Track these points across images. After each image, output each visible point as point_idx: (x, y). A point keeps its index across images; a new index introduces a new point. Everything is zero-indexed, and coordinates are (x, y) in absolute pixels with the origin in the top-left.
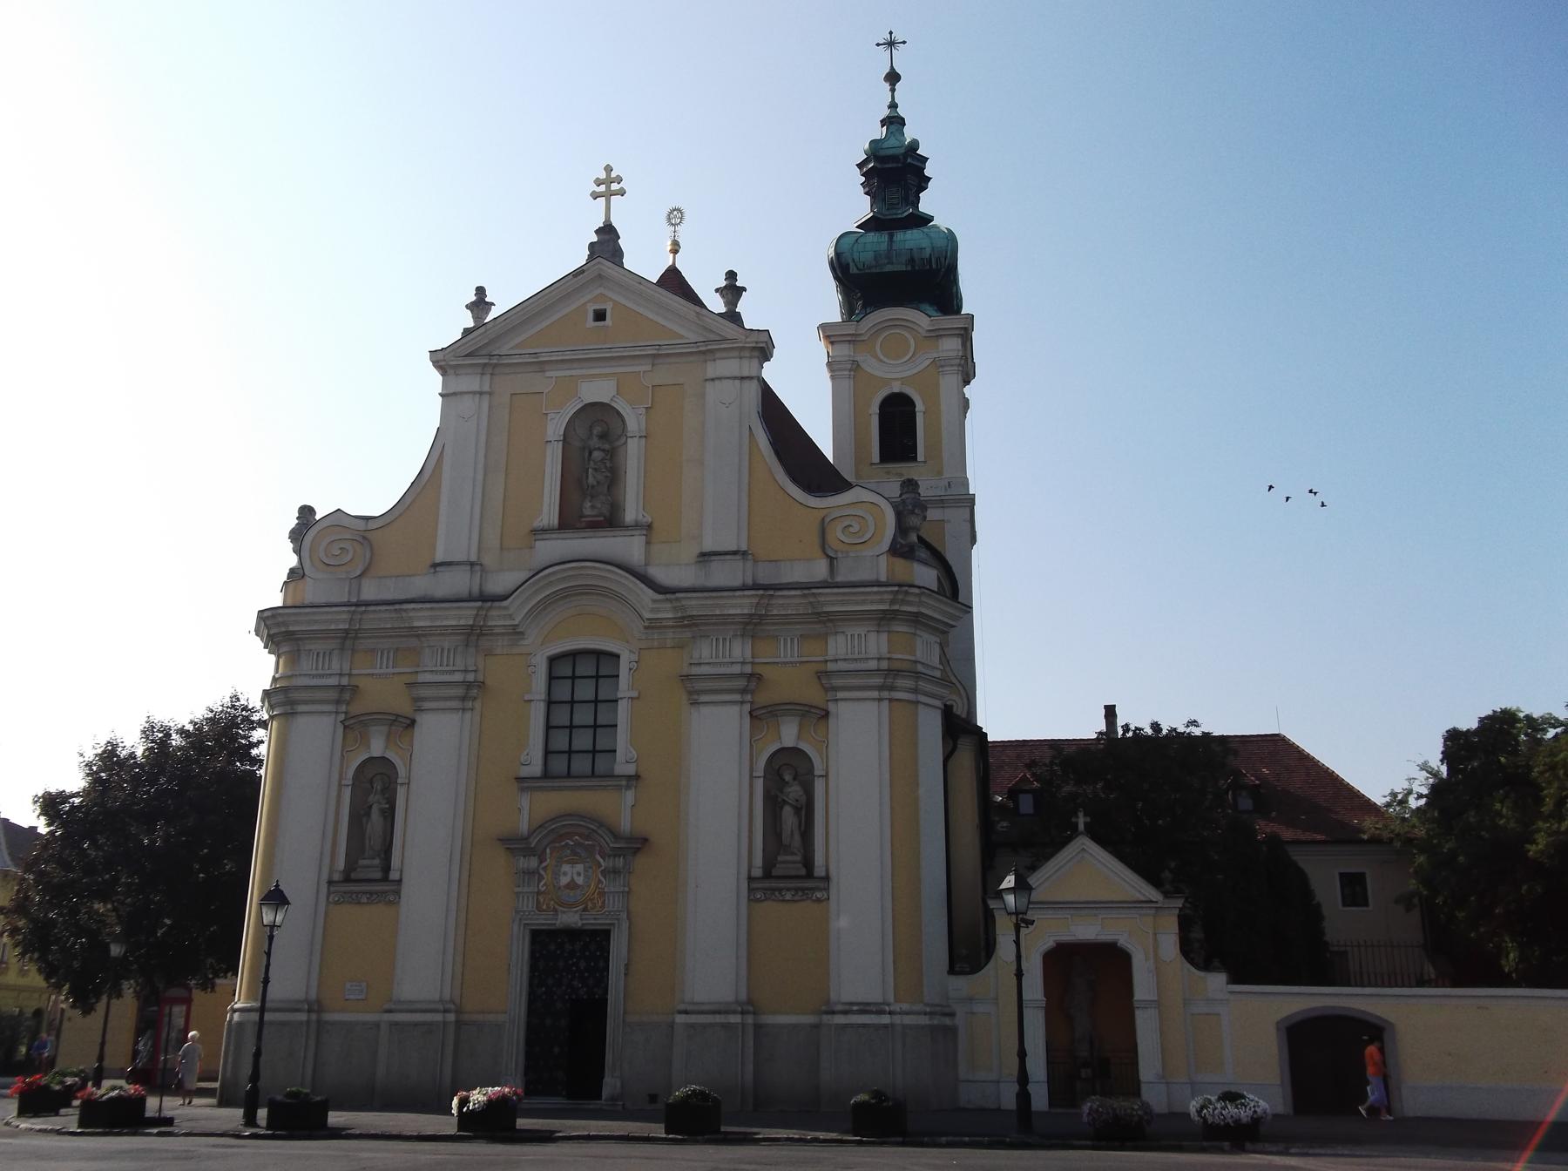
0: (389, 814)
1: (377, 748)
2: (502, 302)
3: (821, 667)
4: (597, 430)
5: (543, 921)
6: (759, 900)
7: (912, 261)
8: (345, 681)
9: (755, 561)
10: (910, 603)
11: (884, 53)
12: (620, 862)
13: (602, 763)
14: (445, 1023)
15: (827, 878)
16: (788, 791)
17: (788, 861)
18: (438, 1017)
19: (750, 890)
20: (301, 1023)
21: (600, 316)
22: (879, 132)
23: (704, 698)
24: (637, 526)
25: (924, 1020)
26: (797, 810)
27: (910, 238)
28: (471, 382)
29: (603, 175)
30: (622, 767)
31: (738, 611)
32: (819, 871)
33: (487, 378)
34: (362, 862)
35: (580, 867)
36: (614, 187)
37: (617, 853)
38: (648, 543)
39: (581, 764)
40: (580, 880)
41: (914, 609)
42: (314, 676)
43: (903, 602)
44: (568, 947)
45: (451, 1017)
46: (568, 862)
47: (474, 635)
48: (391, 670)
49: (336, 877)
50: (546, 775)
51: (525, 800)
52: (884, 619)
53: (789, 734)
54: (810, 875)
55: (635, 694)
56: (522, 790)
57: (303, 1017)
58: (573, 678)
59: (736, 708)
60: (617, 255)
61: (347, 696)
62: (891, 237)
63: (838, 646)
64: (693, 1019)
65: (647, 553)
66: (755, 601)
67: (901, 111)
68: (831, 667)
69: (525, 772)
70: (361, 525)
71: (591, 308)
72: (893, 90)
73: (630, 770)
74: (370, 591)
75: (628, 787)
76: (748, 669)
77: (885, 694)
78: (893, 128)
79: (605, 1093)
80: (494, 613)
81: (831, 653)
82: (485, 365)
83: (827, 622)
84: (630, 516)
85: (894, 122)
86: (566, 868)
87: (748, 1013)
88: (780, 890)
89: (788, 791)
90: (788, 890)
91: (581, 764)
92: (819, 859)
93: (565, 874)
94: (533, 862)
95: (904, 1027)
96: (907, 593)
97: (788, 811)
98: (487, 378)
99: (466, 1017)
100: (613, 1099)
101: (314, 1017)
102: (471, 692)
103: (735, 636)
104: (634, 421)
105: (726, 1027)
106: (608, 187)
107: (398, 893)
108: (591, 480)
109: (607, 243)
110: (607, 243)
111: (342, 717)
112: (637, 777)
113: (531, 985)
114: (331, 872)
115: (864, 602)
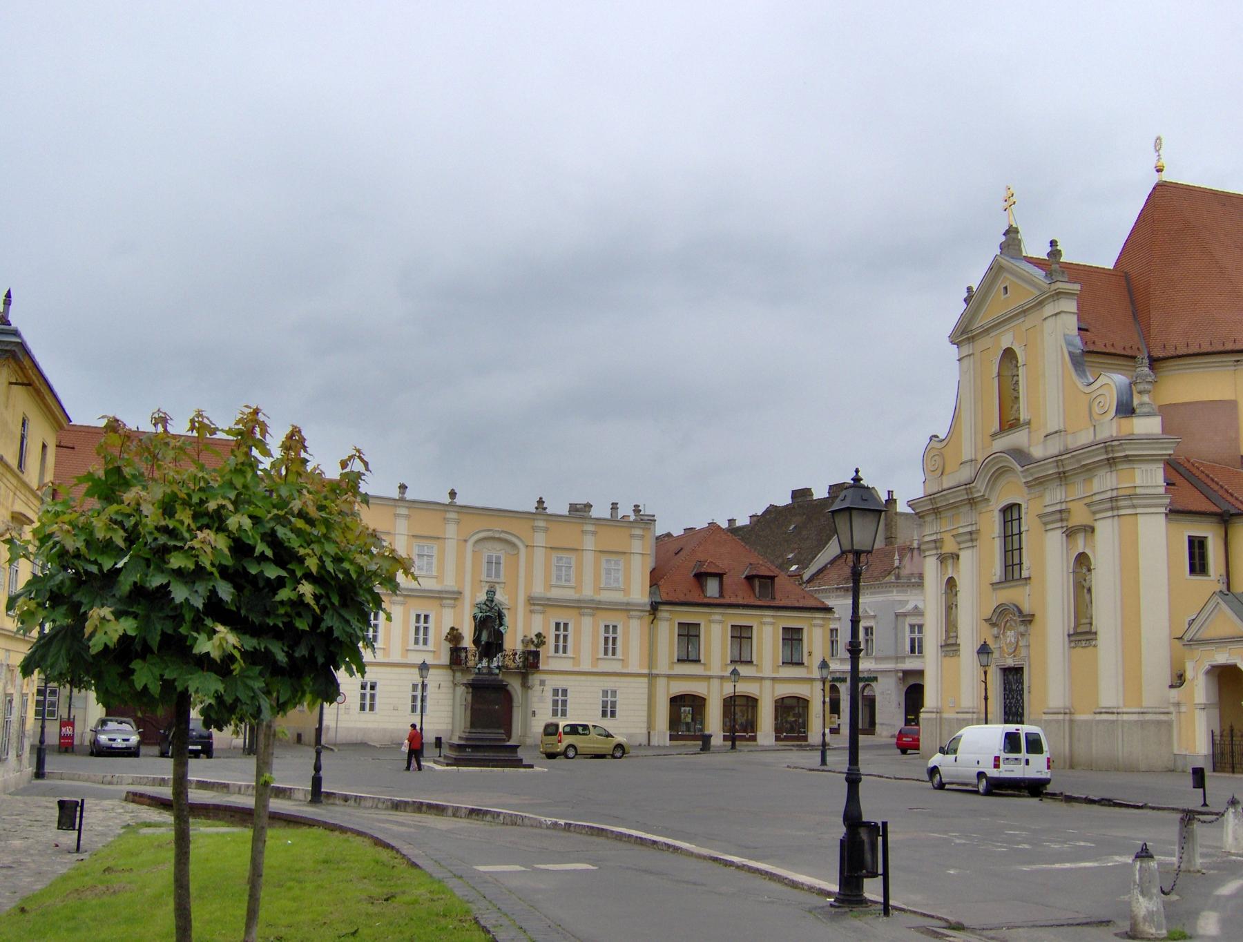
3: (1086, 501)
19: (1070, 642)
21: (1006, 288)
25: (1135, 717)
28: (966, 350)
50: (1006, 580)
52: (1111, 462)
53: (1080, 545)
59: (1059, 532)
60: (1018, 243)
69: (996, 579)
77: (1115, 513)
95: (1123, 721)
105: (1057, 721)
112: (1029, 578)
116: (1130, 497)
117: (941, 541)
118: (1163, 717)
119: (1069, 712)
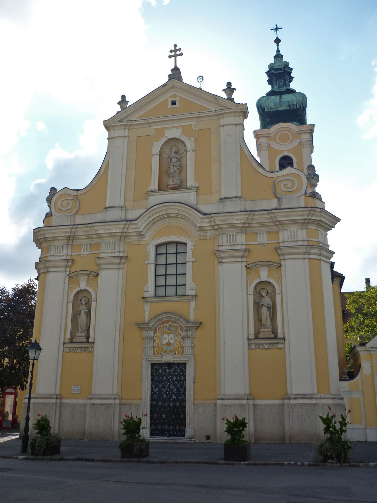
0: (88, 314)
1: (83, 285)
2: (132, 100)
3: (277, 245)
4: (174, 149)
5: (157, 359)
6: (252, 349)
7: (289, 105)
8: (69, 258)
9: (245, 201)
10: (316, 216)
11: (274, 32)
12: (189, 333)
13: (180, 290)
14: (114, 404)
15: (284, 338)
16: (264, 300)
17: (266, 331)
18: (111, 401)
19: (249, 344)
20: (53, 404)
21: (174, 103)
22: (273, 61)
23: (224, 260)
24: (192, 188)
26: (269, 308)
27: (288, 97)
28: (120, 132)
29: (173, 49)
30: (188, 292)
31: (239, 222)
32: (280, 335)
33: (127, 130)
34: (77, 334)
35: (172, 336)
36: (178, 53)
37: (188, 329)
38: (197, 195)
39: (171, 291)
40: (172, 341)
41: (318, 219)
42: (56, 256)
43: (313, 215)
44: (168, 371)
45: (117, 401)
46: (166, 333)
47: (123, 236)
48: (88, 253)
49: (67, 341)
51: (146, 307)
52: (305, 222)
53: (264, 275)
54: (276, 337)
55: (194, 260)
56: (146, 302)
57: (53, 401)
58: (166, 254)
59: (238, 265)
60: (180, 78)
61: (70, 264)
62: (281, 97)
63: (284, 236)
64: (225, 402)
65: (197, 200)
66: (246, 217)
67: (281, 53)
68: (281, 245)
69: (146, 295)
70: (75, 193)
71: (170, 101)
72: (278, 46)
73: (193, 293)
74: (79, 220)
75: (192, 300)
76: (244, 247)
77: (306, 256)
78: (278, 59)
79: (186, 437)
80: (131, 226)
81: (281, 239)
82: (126, 125)
83: (279, 225)
84: (189, 184)
85: (279, 56)
86: (166, 336)
87: (250, 399)
88: (262, 344)
89: (264, 300)
90: (266, 344)
91: (171, 291)
92: (280, 330)
93: (165, 338)
94: (151, 334)
96: (315, 211)
97: (264, 310)
98: (127, 130)
99: (123, 401)
100: (191, 438)
101: (58, 401)
102: (123, 260)
103: (238, 233)
104: (190, 144)
105: (240, 405)
106: (175, 53)
107: (93, 347)
108: (172, 170)
109: (176, 73)
110: (176, 73)
111: (68, 273)
112: (196, 296)
113: (152, 388)
114: (64, 340)
115: (296, 216)
116: (321, 248)
117: (73, 261)
118: (337, 401)
119: (249, 397)
